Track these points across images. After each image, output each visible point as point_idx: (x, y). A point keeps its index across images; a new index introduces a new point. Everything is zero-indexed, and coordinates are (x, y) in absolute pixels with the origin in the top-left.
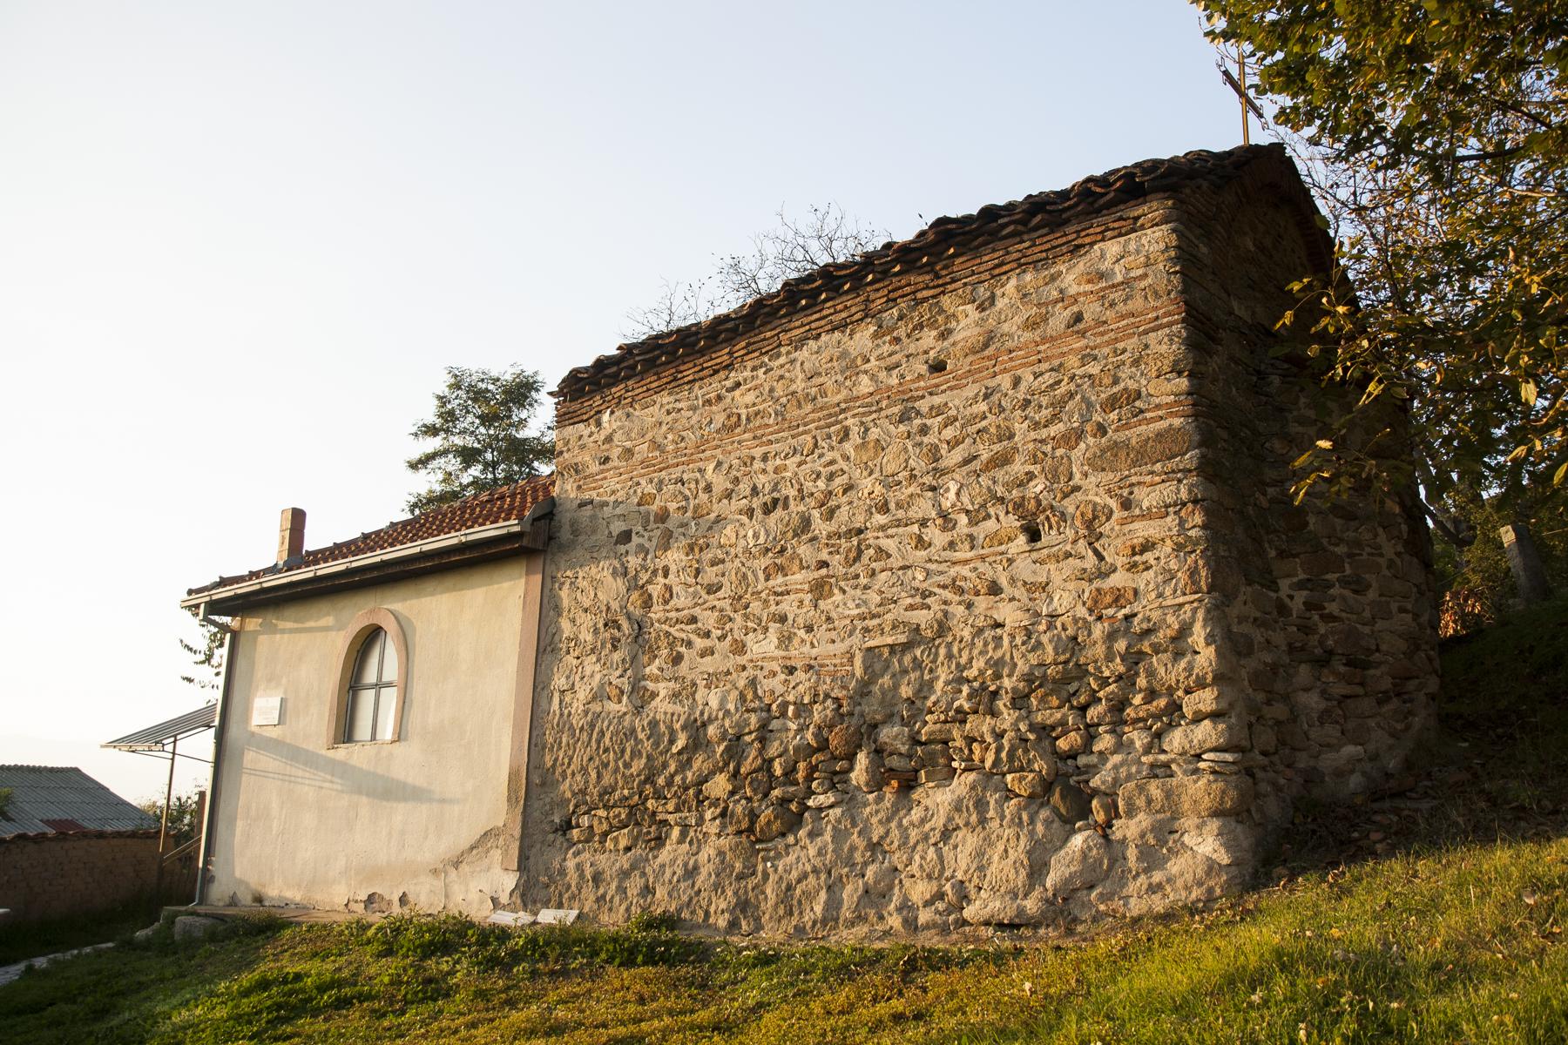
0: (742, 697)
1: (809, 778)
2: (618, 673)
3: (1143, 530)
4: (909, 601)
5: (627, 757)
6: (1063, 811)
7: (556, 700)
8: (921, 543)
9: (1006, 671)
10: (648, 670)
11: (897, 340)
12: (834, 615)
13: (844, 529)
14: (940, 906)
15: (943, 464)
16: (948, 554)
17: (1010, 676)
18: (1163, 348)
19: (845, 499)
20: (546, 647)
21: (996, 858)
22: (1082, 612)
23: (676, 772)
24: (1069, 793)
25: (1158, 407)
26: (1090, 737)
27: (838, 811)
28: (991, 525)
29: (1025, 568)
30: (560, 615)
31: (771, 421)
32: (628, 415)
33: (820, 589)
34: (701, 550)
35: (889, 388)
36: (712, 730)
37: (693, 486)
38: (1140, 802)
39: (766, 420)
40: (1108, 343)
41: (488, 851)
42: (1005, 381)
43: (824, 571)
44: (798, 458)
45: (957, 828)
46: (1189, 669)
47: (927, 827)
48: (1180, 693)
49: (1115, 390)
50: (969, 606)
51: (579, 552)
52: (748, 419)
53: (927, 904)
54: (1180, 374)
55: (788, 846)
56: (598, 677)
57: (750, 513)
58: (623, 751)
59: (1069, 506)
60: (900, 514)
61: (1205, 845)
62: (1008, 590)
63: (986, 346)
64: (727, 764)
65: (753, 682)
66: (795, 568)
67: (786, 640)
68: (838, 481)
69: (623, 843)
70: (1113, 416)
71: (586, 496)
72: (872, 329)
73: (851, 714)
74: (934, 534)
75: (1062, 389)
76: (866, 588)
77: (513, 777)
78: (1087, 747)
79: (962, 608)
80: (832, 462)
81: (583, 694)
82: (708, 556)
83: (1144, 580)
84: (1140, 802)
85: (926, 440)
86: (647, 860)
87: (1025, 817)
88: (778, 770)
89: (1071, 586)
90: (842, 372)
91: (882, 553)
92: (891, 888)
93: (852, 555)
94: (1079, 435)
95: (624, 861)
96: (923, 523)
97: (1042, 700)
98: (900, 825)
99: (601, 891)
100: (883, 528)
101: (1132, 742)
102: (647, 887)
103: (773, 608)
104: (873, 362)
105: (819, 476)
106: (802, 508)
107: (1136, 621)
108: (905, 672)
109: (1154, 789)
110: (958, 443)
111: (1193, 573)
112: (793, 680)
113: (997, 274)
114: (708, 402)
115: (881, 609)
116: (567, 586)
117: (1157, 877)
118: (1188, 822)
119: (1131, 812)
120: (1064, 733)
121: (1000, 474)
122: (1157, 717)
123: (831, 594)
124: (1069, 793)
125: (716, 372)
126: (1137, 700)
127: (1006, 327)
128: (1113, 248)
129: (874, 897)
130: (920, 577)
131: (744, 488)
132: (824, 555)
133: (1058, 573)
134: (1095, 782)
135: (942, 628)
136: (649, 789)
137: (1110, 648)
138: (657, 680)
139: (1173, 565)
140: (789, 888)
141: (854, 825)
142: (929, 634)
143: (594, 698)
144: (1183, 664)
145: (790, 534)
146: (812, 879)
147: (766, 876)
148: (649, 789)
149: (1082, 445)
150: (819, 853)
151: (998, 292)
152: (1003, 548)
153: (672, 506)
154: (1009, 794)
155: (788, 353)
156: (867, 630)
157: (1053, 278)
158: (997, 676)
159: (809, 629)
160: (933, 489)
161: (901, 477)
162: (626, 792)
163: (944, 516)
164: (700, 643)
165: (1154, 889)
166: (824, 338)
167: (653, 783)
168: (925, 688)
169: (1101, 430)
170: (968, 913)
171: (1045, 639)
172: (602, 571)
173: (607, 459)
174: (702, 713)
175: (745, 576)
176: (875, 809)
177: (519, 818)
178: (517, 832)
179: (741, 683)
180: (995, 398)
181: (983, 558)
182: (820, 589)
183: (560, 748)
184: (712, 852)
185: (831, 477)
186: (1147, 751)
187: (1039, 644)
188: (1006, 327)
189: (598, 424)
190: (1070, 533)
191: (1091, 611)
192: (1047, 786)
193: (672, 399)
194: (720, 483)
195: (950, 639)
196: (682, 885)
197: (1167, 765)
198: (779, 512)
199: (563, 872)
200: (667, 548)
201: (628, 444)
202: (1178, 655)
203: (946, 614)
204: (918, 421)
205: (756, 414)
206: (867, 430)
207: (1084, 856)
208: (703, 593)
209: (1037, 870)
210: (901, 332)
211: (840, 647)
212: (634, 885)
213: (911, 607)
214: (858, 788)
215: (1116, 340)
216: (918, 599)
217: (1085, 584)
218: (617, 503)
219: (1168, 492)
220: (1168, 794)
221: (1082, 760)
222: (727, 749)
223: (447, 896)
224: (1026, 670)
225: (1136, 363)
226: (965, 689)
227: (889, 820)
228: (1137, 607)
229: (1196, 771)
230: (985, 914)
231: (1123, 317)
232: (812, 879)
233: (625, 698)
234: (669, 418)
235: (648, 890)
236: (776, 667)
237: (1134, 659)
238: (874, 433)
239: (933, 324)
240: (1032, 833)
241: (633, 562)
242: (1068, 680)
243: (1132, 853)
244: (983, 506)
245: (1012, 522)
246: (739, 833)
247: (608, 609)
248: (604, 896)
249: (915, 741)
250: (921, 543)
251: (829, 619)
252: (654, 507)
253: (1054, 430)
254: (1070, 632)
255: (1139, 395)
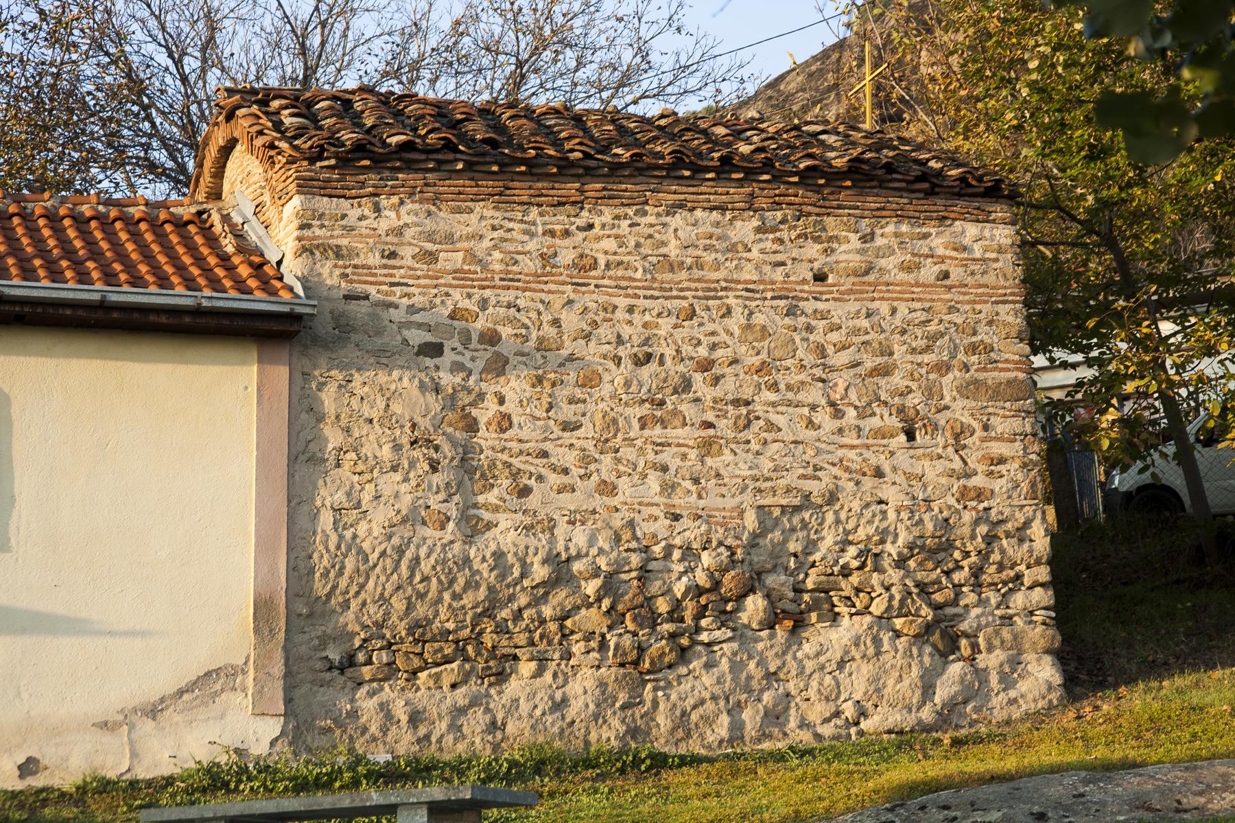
0: (617, 539)
1: (699, 616)
2: (442, 496)
3: (997, 449)
4: (801, 471)
5: (458, 588)
6: (940, 646)
7: (326, 519)
8: (810, 424)
9: (890, 539)
10: (481, 499)
11: (781, 241)
12: (722, 472)
13: (730, 397)
14: (839, 722)
15: (830, 362)
16: (837, 438)
17: (893, 543)
18: (1010, 319)
19: (728, 370)
20: (300, 456)
21: (890, 682)
22: (952, 501)
23: (528, 606)
24: (943, 636)
25: (1007, 361)
26: (958, 595)
27: (735, 645)
28: (875, 422)
29: (902, 459)
30: (321, 418)
31: (639, 275)
32: (429, 214)
33: (707, 447)
34: (554, 385)
35: (773, 283)
36: (577, 566)
37: (534, 315)
38: (997, 642)
39: (630, 273)
40: (969, 302)
41: (216, 694)
42: (884, 308)
43: (711, 432)
44: (673, 320)
45: (853, 659)
46: (1031, 551)
47: (822, 659)
48: (1023, 567)
49: (974, 339)
50: (858, 483)
51: (349, 353)
52: (608, 266)
53: (827, 721)
54: (1021, 340)
55: (679, 676)
56: (408, 499)
57: (618, 360)
58: (452, 582)
59: (941, 419)
60: (790, 395)
61: (1043, 674)
62: (890, 477)
63: (867, 273)
64: (599, 600)
65: (631, 524)
66: (677, 422)
67: (669, 488)
68: (720, 353)
69: (446, 682)
70: (974, 359)
71: (360, 288)
72: (756, 223)
73: (742, 561)
74: (823, 417)
75: (932, 328)
76: (758, 453)
77: (263, 608)
78: (955, 603)
79: (852, 484)
80: (713, 334)
81: (380, 516)
82: (563, 393)
83: (999, 485)
84: (997, 642)
85: (812, 338)
86: (488, 695)
87: (915, 651)
88: (662, 606)
89: (944, 480)
90: (724, 253)
91: (771, 427)
92: (787, 708)
93: (741, 422)
94: (949, 368)
95: (461, 696)
96: (813, 408)
97: (920, 564)
98: (795, 658)
99: (422, 731)
100: (774, 404)
101: (988, 599)
102: (493, 723)
103: (651, 456)
104: (755, 251)
105: (699, 343)
106: (681, 368)
107: (993, 512)
108: (793, 530)
109: (1006, 633)
110: (844, 348)
111: (1033, 485)
112: (679, 527)
113: (878, 215)
114: (552, 233)
115: (774, 475)
116: (332, 388)
117: (1012, 694)
118: (1029, 657)
119: (990, 649)
120: (940, 590)
121: (882, 382)
122: (1005, 583)
123: (720, 453)
124: (943, 636)
125: (560, 204)
126: (993, 568)
127: (883, 262)
128: (972, 230)
129: (775, 716)
130: (811, 452)
131: (604, 332)
132: (710, 416)
133: (932, 471)
134: (964, 626)
135: (832, 498)
136: (488, 625)
137: (973, 530)
138: (496, 509)
139: (1020, 477)
140: (684, 713)
141: (750, 657)
142: (819, 501)
143: (404, 521)
144: (1026, 546)
145: (669, 391)
146: (710, 706)
147: (655, 704)
148: (488, 625)
149: (950, 376)
150: (719, 682)
151: (878, 232)
152: (885, 441)
153: (506, 331)
154: (898, 634)
155: (658, 215)
156: (760, 491)
157: (926, 236)
158: (882, 542)
159: (696, 481)
160: (823, 381)
161: (789, 363)
162: (451, 626)
163: (832, 404)
164: (554, 479)
165: (1012, 702)
166: (699, 213)
167: (492, 617)
168: (811, 546)
169: (966, 367)
170: (864, 725)
171: (926, 517)
172: (404, 381)
173: (393, 255)
174: (567, 549)
175: (615, 421)
176: (770, 644)
177: (279, 655)
178: (278, 669)
179: (617, 523)
180: (875, 319)
181: (868, 447)
182: (707, 447)
183: (340, 573)
184: (590, 684)
185: (713, 347)
186: (998, 607)
187: (921, 521)
188: (883, 262)
189: (377, 209)
190: (940, 440)
191: (958, 501)
192: (928, 628)
193: (497, 214)
194: (571, 321)
195: (837, 507)
196: (549, 719)
197: (1011, 617)
198: (653, 366)
199: (354, 714)
200: (501, 372)
201: (429, 246)
202: (1021, 541)
203: (837, 487)
204: (802, 319)
205: (620, 263)
206: (751, 314)
207: (962, 680)
208: (557, 432)
209: (928, 690)
210: (785, 235)
211: (730, 503)
212: (475, 722)
213: (804, 477)
214: (748, 626)
215: (974, 302)
216: (810, 470)
217: (953, 480)
218: (412, 309)
219: (1016, 424)
220: (1015, 637)
221: (950, 611)
222: (604, 586)
223: (134, 755)
224: (911, 539)
225: (990, 323)
226: (852, 551)
227: (784, 653)
228: (992, 503)
229: (1031, 622)
230: (889, 724)
231: (981, 286)
232: (710, 706)
233: (451, 526)
234: (496, 234)
235: (493, 726)
236: (655, 511)
237: (990, 539)
238: (759, 319)
239: (817, 240)
240: (921, 662)
241: (448, 379)
242: (938, 549)
243: (994, 679)
244: (869, 404)
245: (894, 422)
246: (622, 665)
247: (414, 426)
248: (427, 737)
249: (798, 590)
250: (810, 424)
251: (718, 475)
252: (480, 324)
253: (927, 358)
254: (946, 514)
255: (992, 350)
